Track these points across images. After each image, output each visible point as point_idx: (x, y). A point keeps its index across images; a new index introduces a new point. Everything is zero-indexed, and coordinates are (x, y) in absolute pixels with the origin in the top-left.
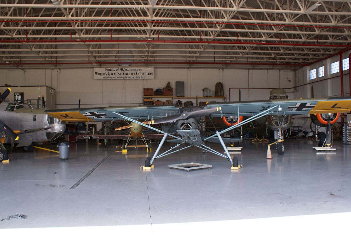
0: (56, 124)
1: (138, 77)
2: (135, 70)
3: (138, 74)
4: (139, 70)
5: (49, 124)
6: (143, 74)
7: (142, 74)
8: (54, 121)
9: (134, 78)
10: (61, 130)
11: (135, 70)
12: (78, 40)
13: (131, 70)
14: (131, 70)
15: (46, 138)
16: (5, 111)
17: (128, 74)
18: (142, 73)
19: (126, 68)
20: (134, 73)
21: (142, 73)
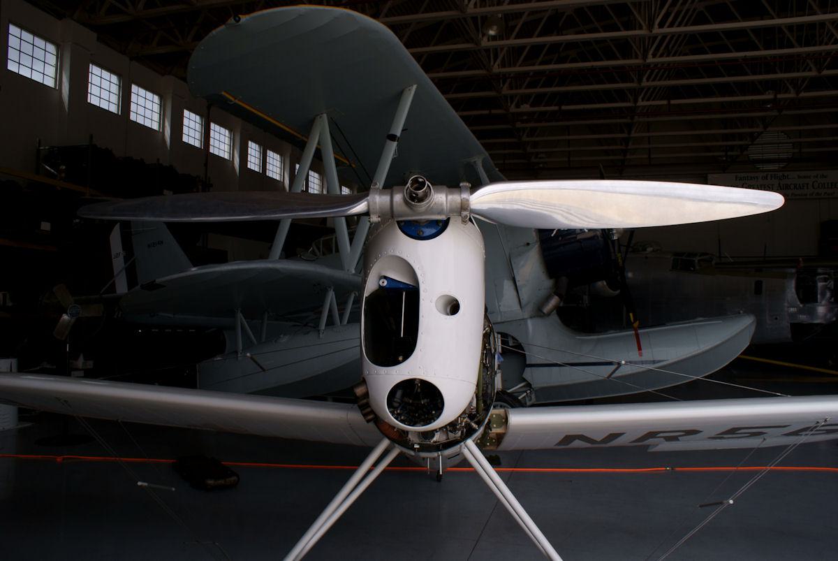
0: (823, 302)
1: (818, 194)
2: (809, 177)
3: (816, 185)
4: (819, 176)
5: (801, 303)
6: (830, 186)
7: (826, 186)
8: (819, 296)
9: (806, 195)
10: (834, 319)
11: (809, 177)
12: (769, 106)
13: (799, 177)
14: (799, 177)
15: (790, 336)
16: (670, 270)
17: (792, 187)
18: (826, 185)
19: (786, 174)
20: (807, 184)
21: (826, 185)
